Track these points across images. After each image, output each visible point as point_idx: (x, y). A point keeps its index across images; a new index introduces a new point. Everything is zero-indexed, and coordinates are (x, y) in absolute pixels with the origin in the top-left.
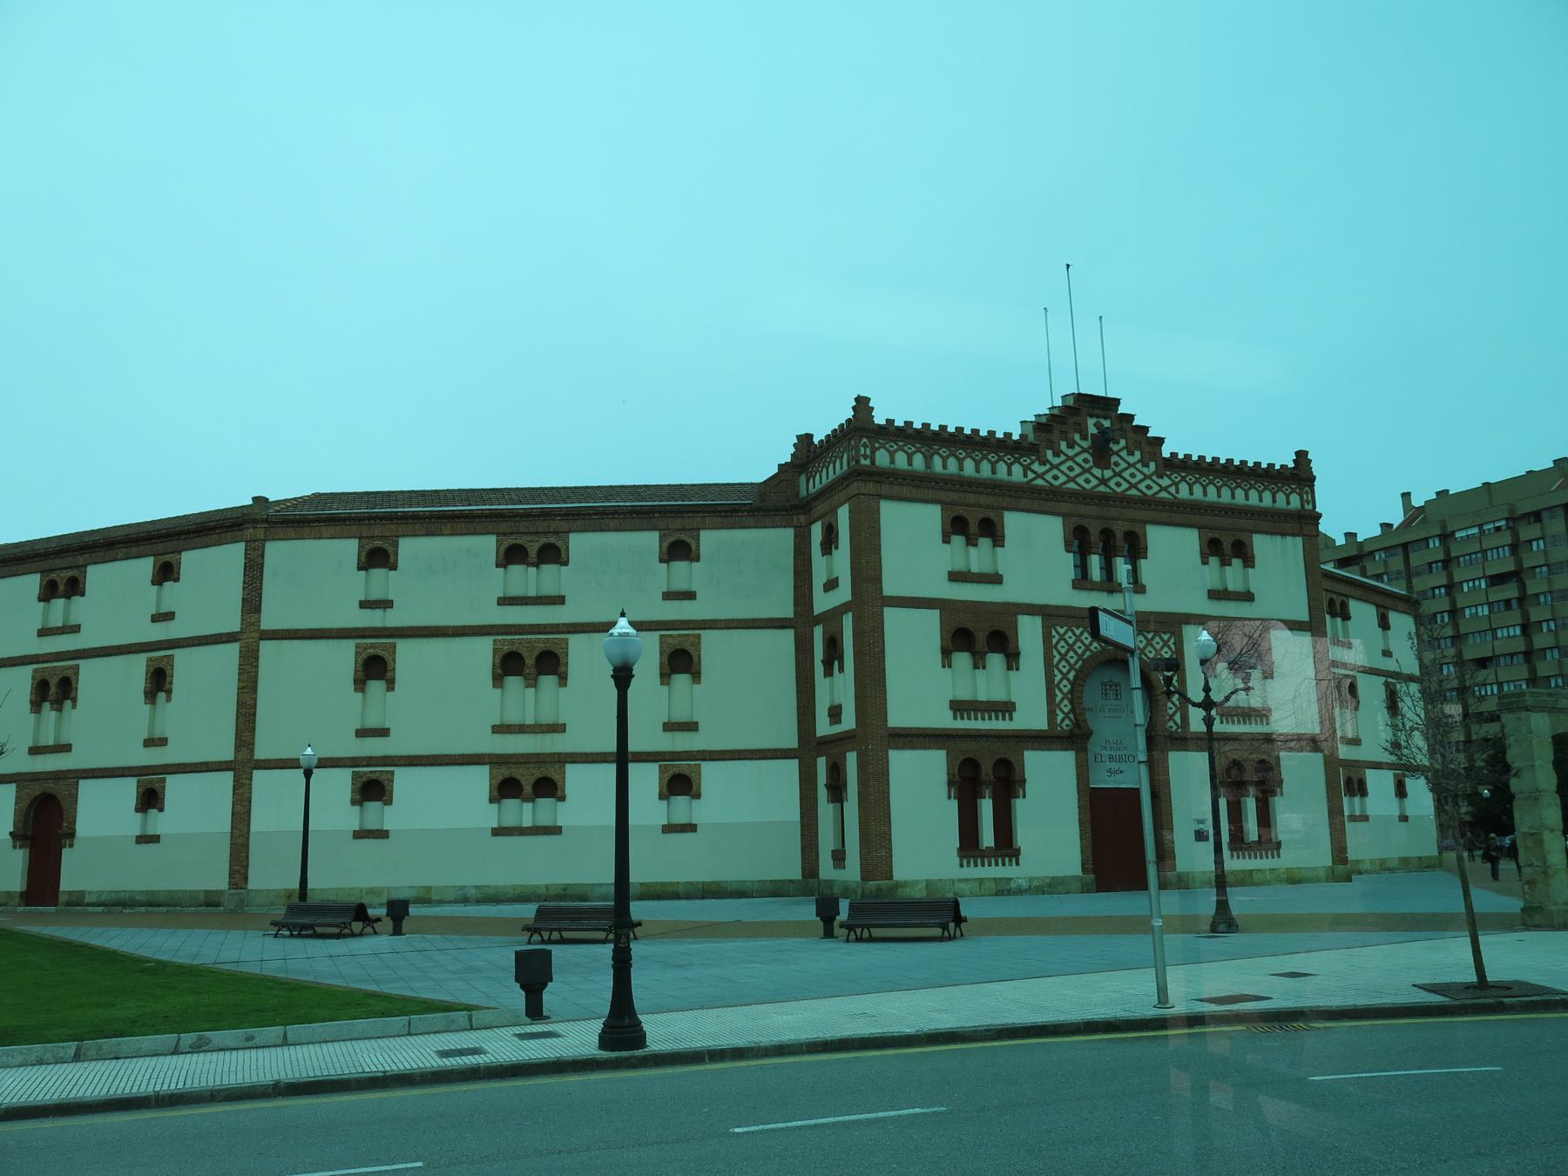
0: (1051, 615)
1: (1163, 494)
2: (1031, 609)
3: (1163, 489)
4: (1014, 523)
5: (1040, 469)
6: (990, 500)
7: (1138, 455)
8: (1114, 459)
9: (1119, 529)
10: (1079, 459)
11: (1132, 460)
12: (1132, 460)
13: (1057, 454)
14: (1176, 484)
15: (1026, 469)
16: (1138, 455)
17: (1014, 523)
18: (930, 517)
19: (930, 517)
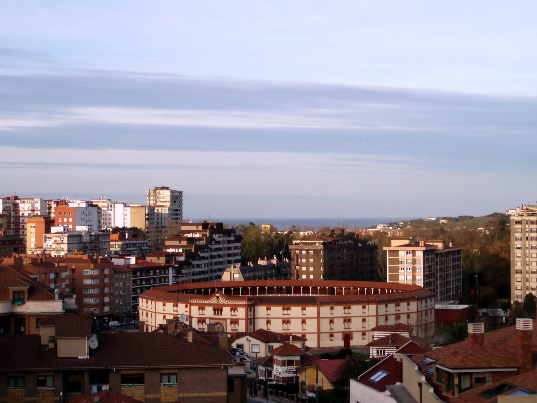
0: (210, 319)
1: (226, 303)
2: (208, 318)
3: (226, 302)
4: (206, 308)
5: (210, 301)
6: (203, 305)
7: (223, 298)
8: (220, 299)
9: (219, 308)
10: (215, 300)
11: (222, 299)
12: (222, 299)
13: (212, 299)
14: (228, 302)
15: (208, 301)
16: (223, 298)
17: (206, 308)
18: (197, 307)
19: (197, 307)
